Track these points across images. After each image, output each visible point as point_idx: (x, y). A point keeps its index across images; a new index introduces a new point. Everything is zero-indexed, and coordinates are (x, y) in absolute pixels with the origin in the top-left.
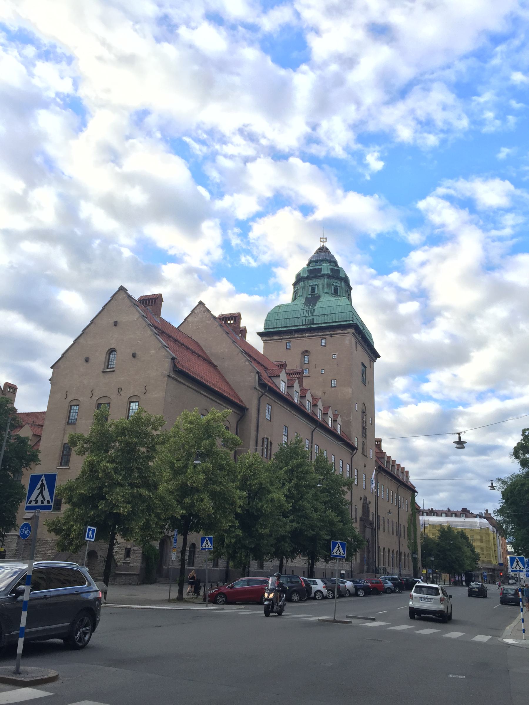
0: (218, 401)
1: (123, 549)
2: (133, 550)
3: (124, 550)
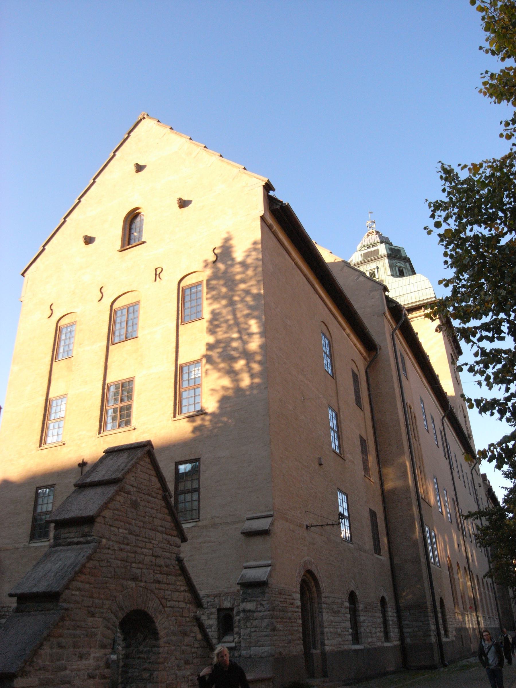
0: (340, 319)
1: (211, 613)
2: (244, 611)
3: (215, 616)
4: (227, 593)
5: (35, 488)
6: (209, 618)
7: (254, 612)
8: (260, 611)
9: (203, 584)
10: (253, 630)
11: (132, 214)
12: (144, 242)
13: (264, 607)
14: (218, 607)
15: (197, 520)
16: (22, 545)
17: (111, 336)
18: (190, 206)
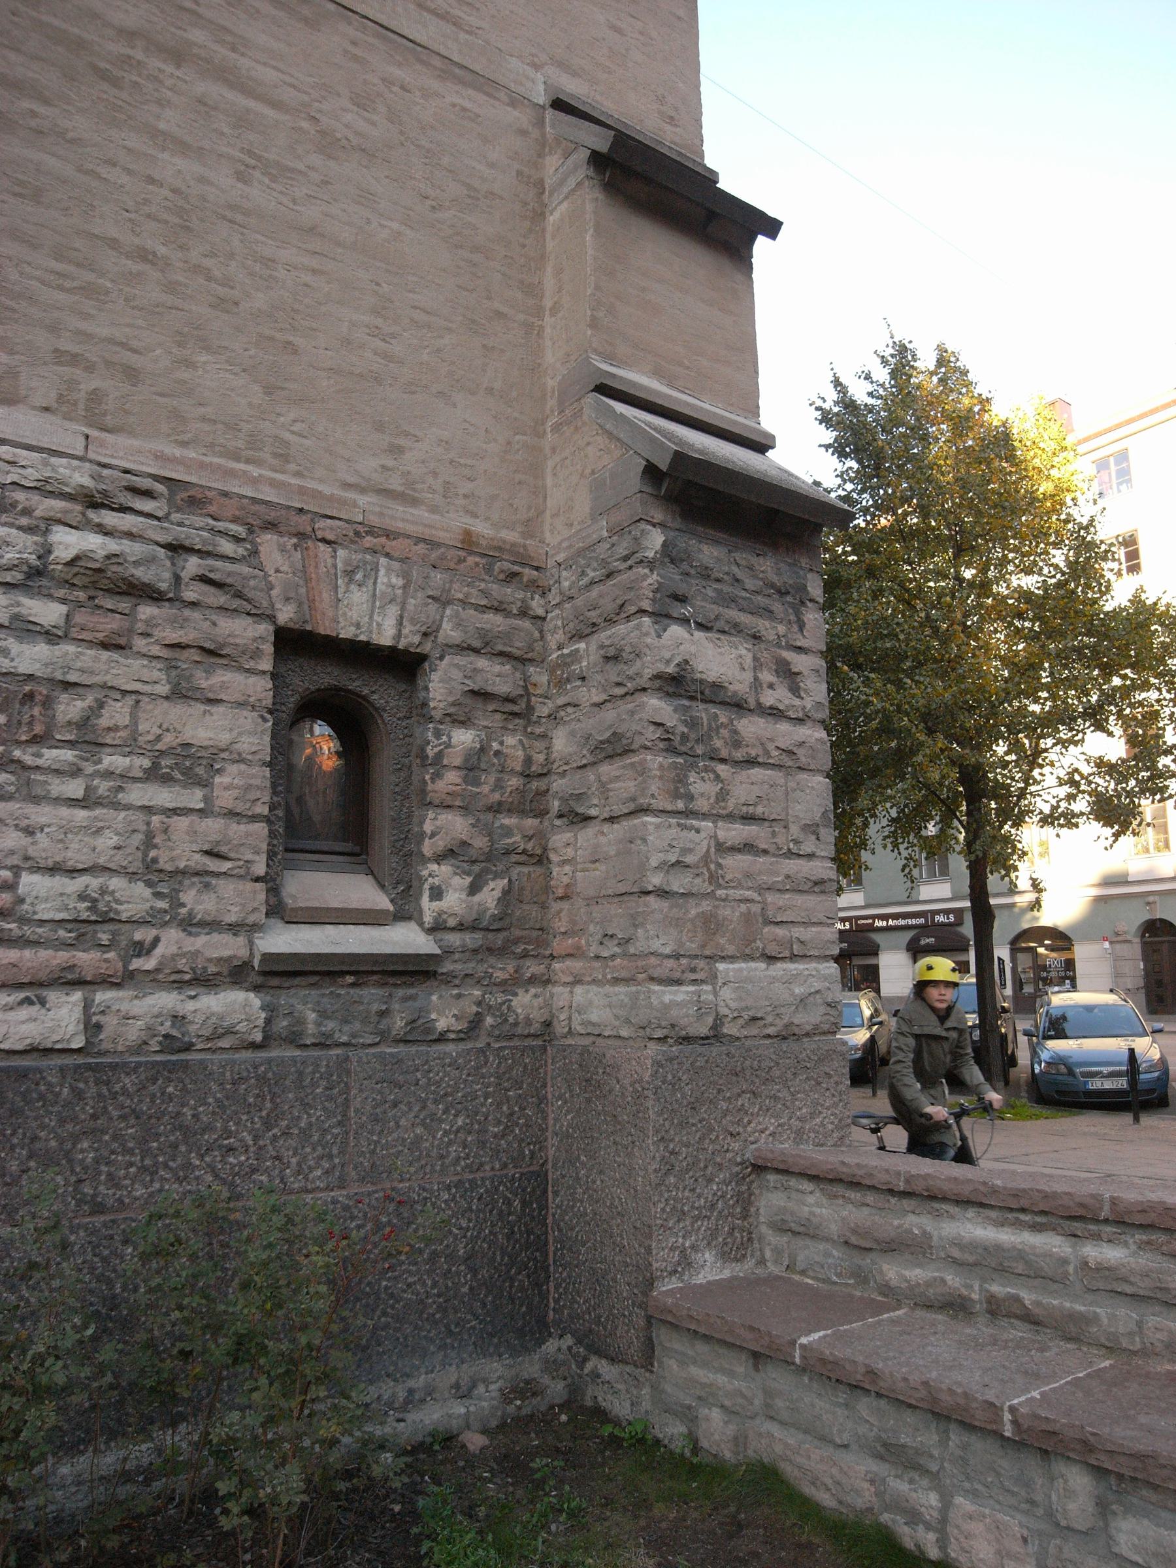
4: (372, 531)
6: (180, 693)
7: (738, 706)
8: (775, 713)
9: (132, 375)
10: (734, 833)
13: (795, 690)
14: (286, 615)
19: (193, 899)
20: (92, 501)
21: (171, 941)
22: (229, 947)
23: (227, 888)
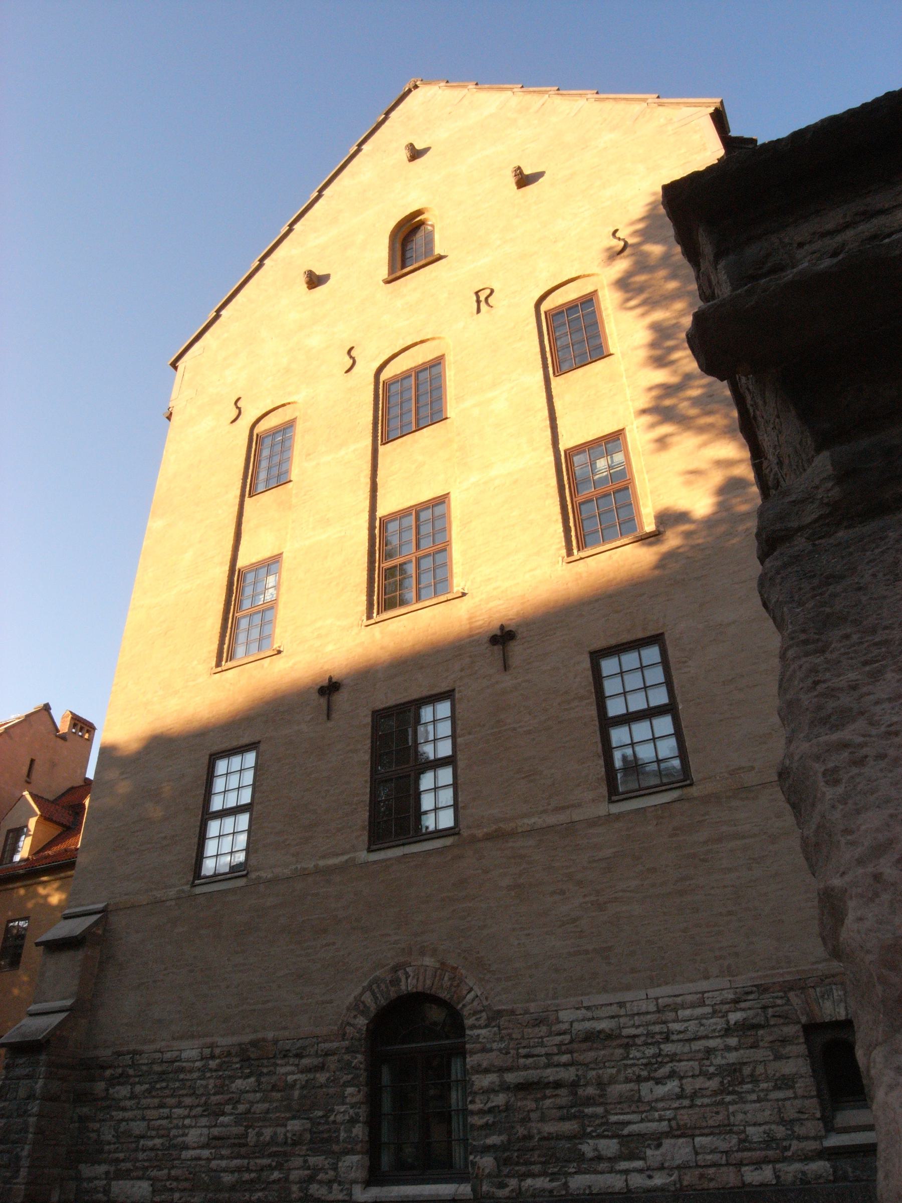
1: (784, 1041)
5: (208, 757)
6: (778, 1057)
9: (737, 954)
11: (409, 224)
12: (440, 258)
14: (804, 1019)
15: (688, 782)
16: (172, 893)
17: (380, 428)
18: (541, 180)
19: (799, 1130)
20: (736, 1001)
21: (795, 1145)
22: (812, 1145)
23: (809, 1124)
